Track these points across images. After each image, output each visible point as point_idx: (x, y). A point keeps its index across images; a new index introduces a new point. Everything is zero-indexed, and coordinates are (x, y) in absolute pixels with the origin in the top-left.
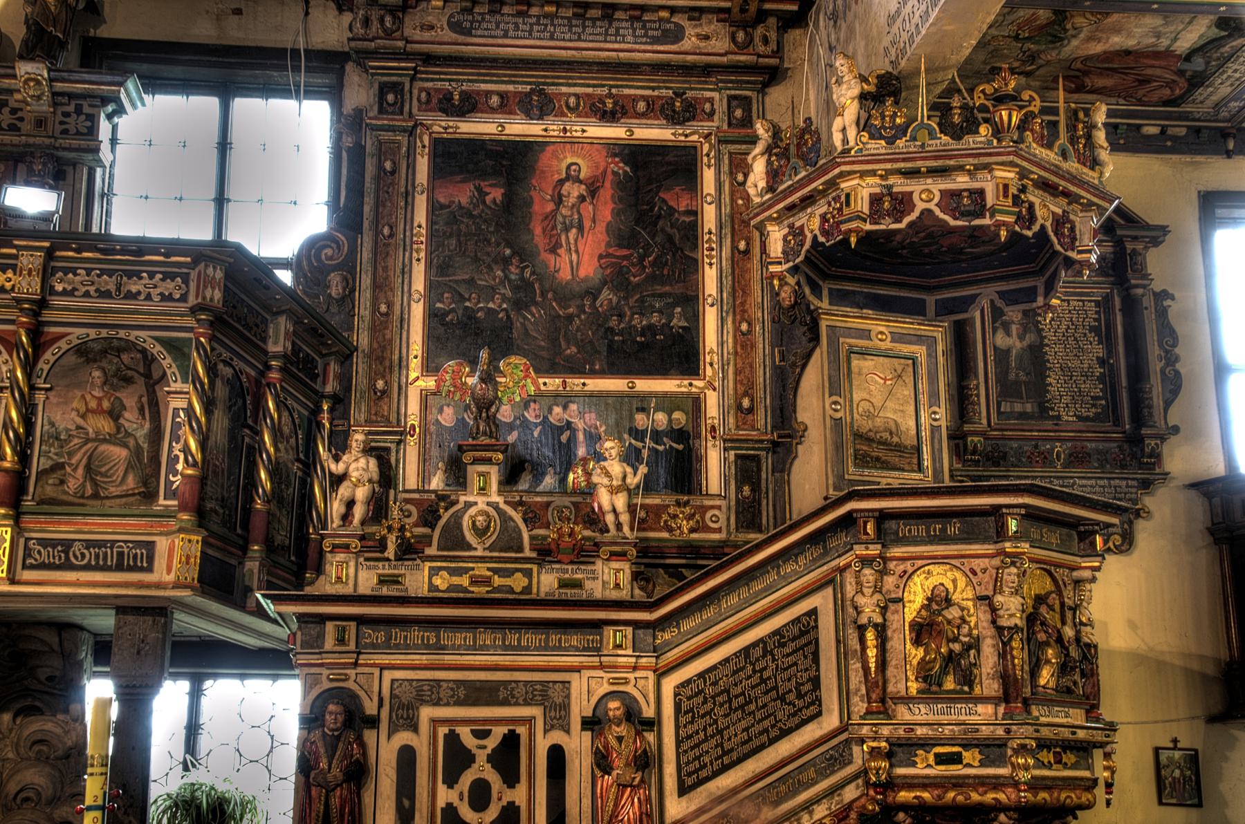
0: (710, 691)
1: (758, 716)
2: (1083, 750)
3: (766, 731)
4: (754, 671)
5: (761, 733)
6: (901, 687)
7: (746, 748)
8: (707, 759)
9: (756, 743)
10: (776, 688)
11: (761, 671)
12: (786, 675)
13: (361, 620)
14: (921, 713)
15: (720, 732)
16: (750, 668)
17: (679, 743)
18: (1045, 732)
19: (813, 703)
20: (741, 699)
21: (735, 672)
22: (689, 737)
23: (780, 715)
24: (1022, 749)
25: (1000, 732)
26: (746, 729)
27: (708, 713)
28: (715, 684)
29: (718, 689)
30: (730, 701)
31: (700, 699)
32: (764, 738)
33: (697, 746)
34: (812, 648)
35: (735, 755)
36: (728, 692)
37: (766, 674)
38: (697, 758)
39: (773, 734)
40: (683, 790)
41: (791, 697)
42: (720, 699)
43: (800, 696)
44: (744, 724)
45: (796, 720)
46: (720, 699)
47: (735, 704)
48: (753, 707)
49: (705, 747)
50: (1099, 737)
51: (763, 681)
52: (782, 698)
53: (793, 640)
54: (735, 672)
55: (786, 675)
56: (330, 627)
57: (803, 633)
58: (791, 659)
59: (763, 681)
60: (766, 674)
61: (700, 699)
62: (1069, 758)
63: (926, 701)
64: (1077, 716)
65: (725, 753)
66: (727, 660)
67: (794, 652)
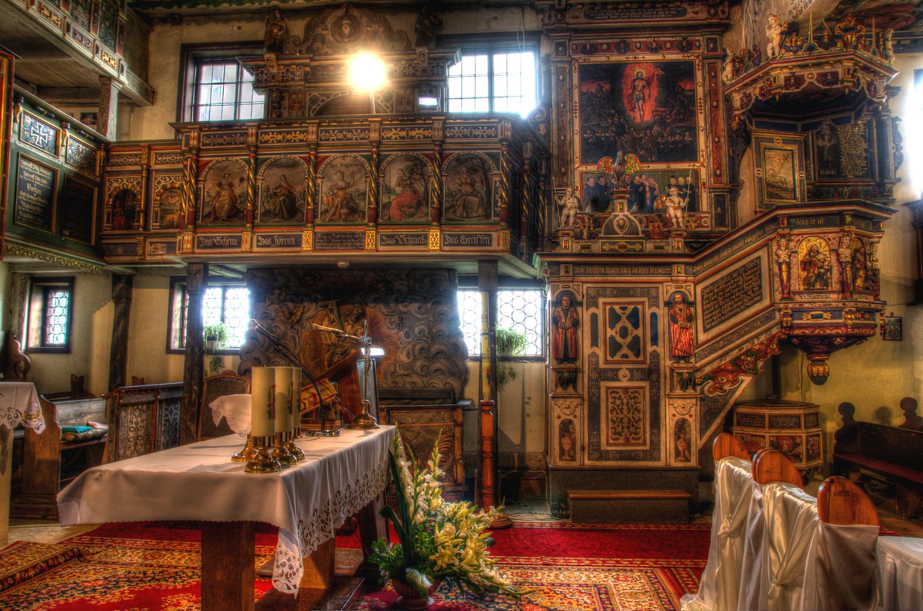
2: (871, 312)
4: (734, 282)
6: (797, 287)
10: (743, 289)
11: (737, 282)
12: (747, 284)
13: (574, 264)
14: (806, 298)
18: (859, 305)
21: (726, 283)
24: (851, 312)
25: (841, 305)
37: (739, 284)
50: (880, 307)
51: (738, 286)
54: (726, 283)
55: (747, 284)
56: (562, 266)
59: (738, 286)
60: (739, 284)
62: (867, 316)
63: (808, 293)
64: (871, 299)
66: (723, 278)
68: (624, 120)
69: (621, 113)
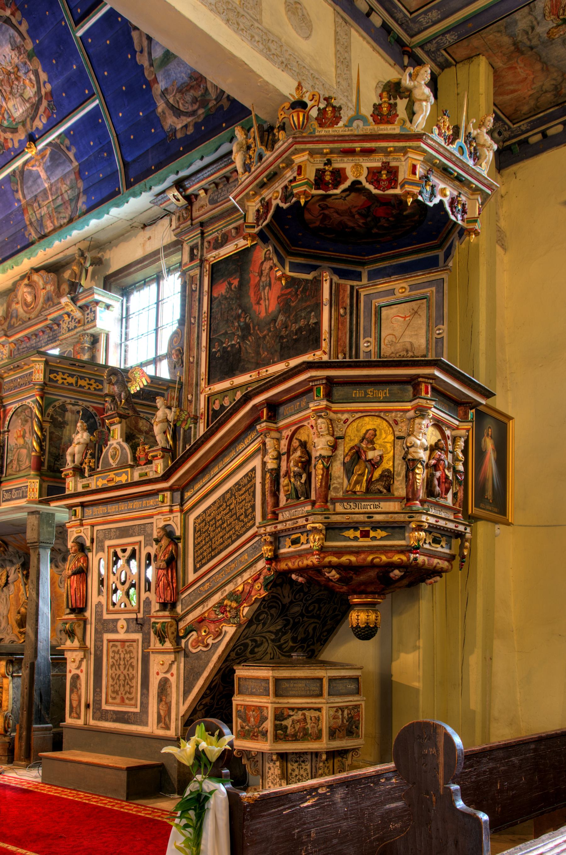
0: (208, 519)
1: (227, 529)
3: (231, 537)
5: (228, 538)
7: (222, 547)
8: (205, 554)
9: (226, 543)
15: (211, 540)
16: (225, 505)
17: (195, 546)
19: (252, 519)
20: (220, 522)
22: (199, 543)
23: (237, 528)
26: (222, 537)
27: (206, 531)
28: (209, 515)
29: (211, 518)
30: (216, 523)
31: (204, 523)
32: (230, 541)
33: (201, 548)
34: (252, 489)
35: (217, 551)
36: (215, 518)
38: (202, 554)
39: (233, 538)
40: (195, 570)
41: (242, 517)
42: (211, 523)
43: (246, 516)
44: (221, 534)
45: (244, 529)
46: (211, 523)
47: (218, 524)
48: (225, 525)
49: (205, 548)
52: (238, 519)
53: (244, 486)
57: (249, 481)
58: (243, 497)
61: (204, 523)
65: (213, 550)
67: (245, 492)
68: (250, 319)
69: (246, 310)
